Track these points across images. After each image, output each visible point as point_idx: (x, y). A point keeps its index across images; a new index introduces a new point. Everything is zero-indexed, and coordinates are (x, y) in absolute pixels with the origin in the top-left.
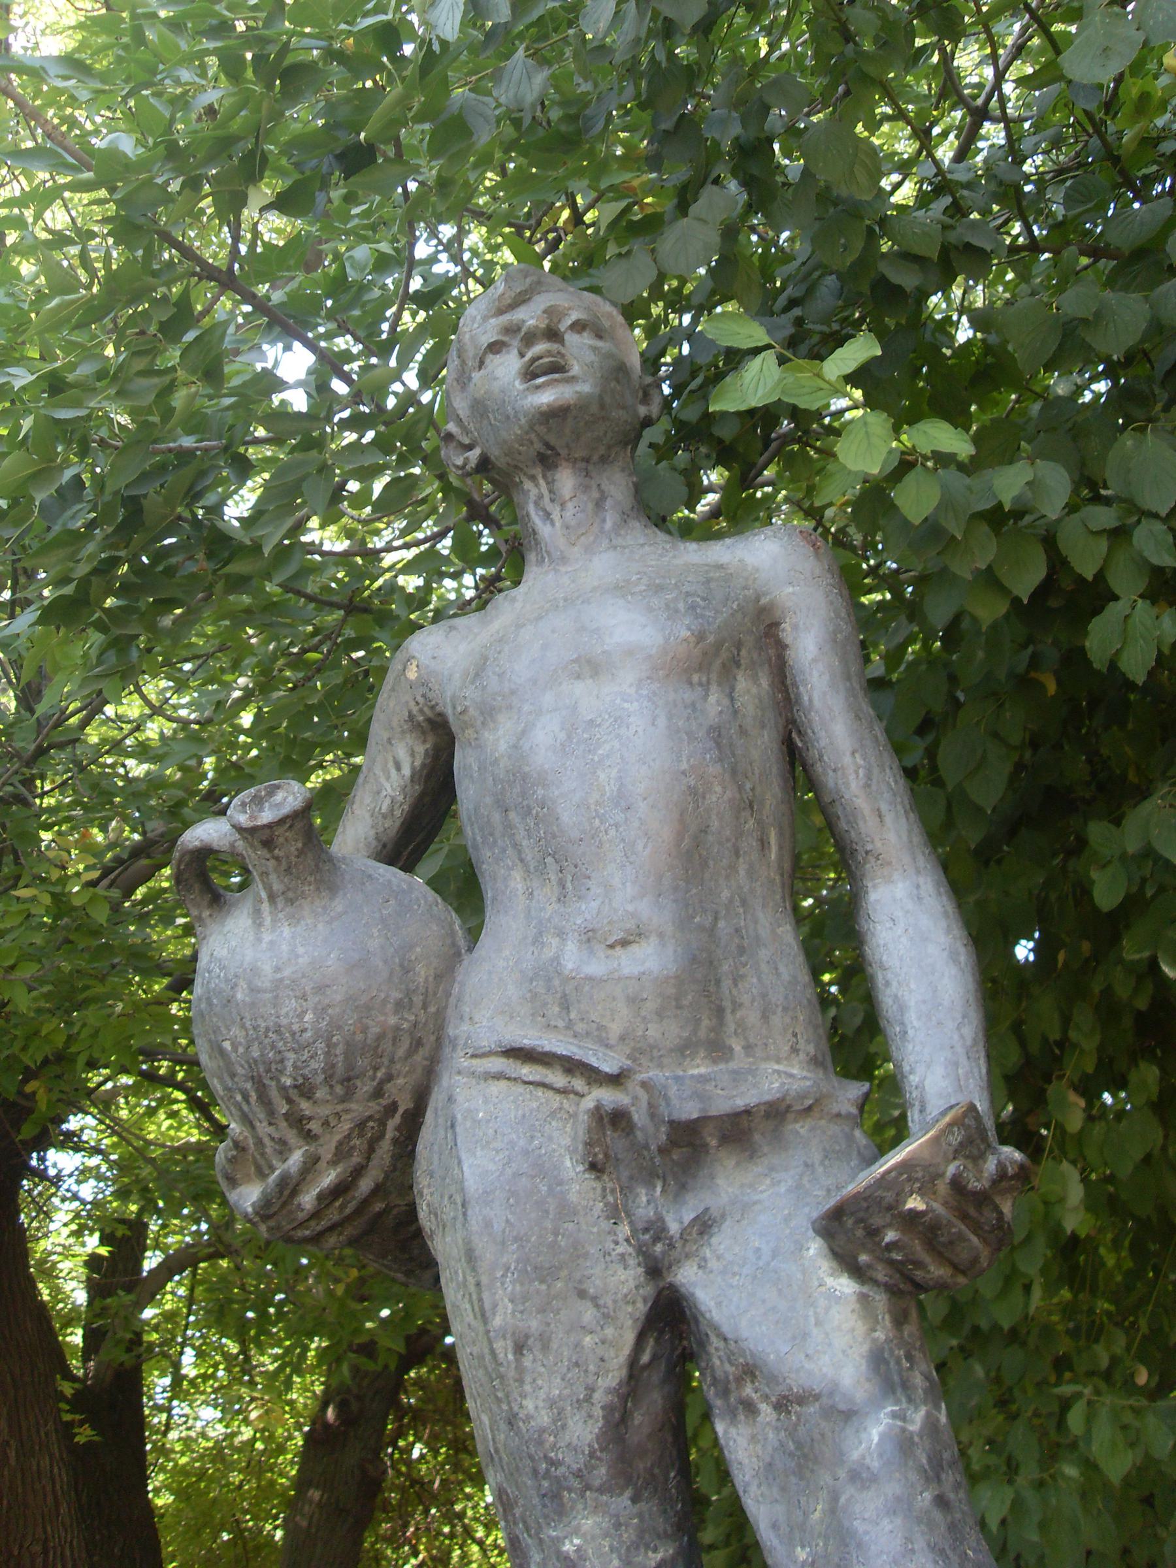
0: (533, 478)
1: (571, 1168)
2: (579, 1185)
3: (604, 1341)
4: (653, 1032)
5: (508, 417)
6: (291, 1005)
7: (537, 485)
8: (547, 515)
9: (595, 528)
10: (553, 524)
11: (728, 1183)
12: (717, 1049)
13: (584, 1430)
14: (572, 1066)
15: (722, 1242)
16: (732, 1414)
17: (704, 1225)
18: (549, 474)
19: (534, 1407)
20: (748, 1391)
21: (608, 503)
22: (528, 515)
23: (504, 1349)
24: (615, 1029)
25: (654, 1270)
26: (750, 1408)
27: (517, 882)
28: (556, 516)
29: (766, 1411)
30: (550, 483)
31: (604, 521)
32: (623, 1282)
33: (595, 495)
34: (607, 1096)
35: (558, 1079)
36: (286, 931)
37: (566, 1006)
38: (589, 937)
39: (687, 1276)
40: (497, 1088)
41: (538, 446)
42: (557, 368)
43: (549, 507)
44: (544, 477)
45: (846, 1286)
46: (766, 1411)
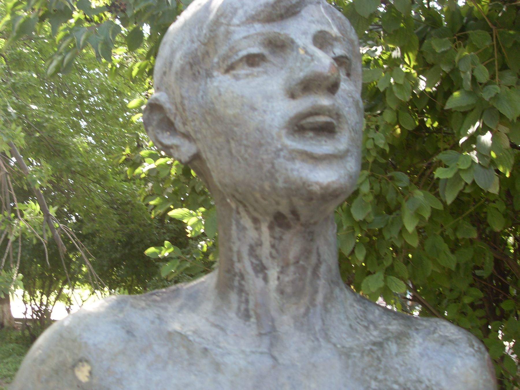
0: (255, 221)
5: (260, 167)
7: (257, 229)
8: (261, 269)
9: (305, 300)
10: (266, 279)
18: (277, 229)
21: (323, 269)
22: (239, 253)
28: (273, 273)
30: (276, 240)
31: (316, 292)
33: (313, 260)
41: (284, 208)
42: (327, 130)
43: (267, 262)
44: (271, 227)
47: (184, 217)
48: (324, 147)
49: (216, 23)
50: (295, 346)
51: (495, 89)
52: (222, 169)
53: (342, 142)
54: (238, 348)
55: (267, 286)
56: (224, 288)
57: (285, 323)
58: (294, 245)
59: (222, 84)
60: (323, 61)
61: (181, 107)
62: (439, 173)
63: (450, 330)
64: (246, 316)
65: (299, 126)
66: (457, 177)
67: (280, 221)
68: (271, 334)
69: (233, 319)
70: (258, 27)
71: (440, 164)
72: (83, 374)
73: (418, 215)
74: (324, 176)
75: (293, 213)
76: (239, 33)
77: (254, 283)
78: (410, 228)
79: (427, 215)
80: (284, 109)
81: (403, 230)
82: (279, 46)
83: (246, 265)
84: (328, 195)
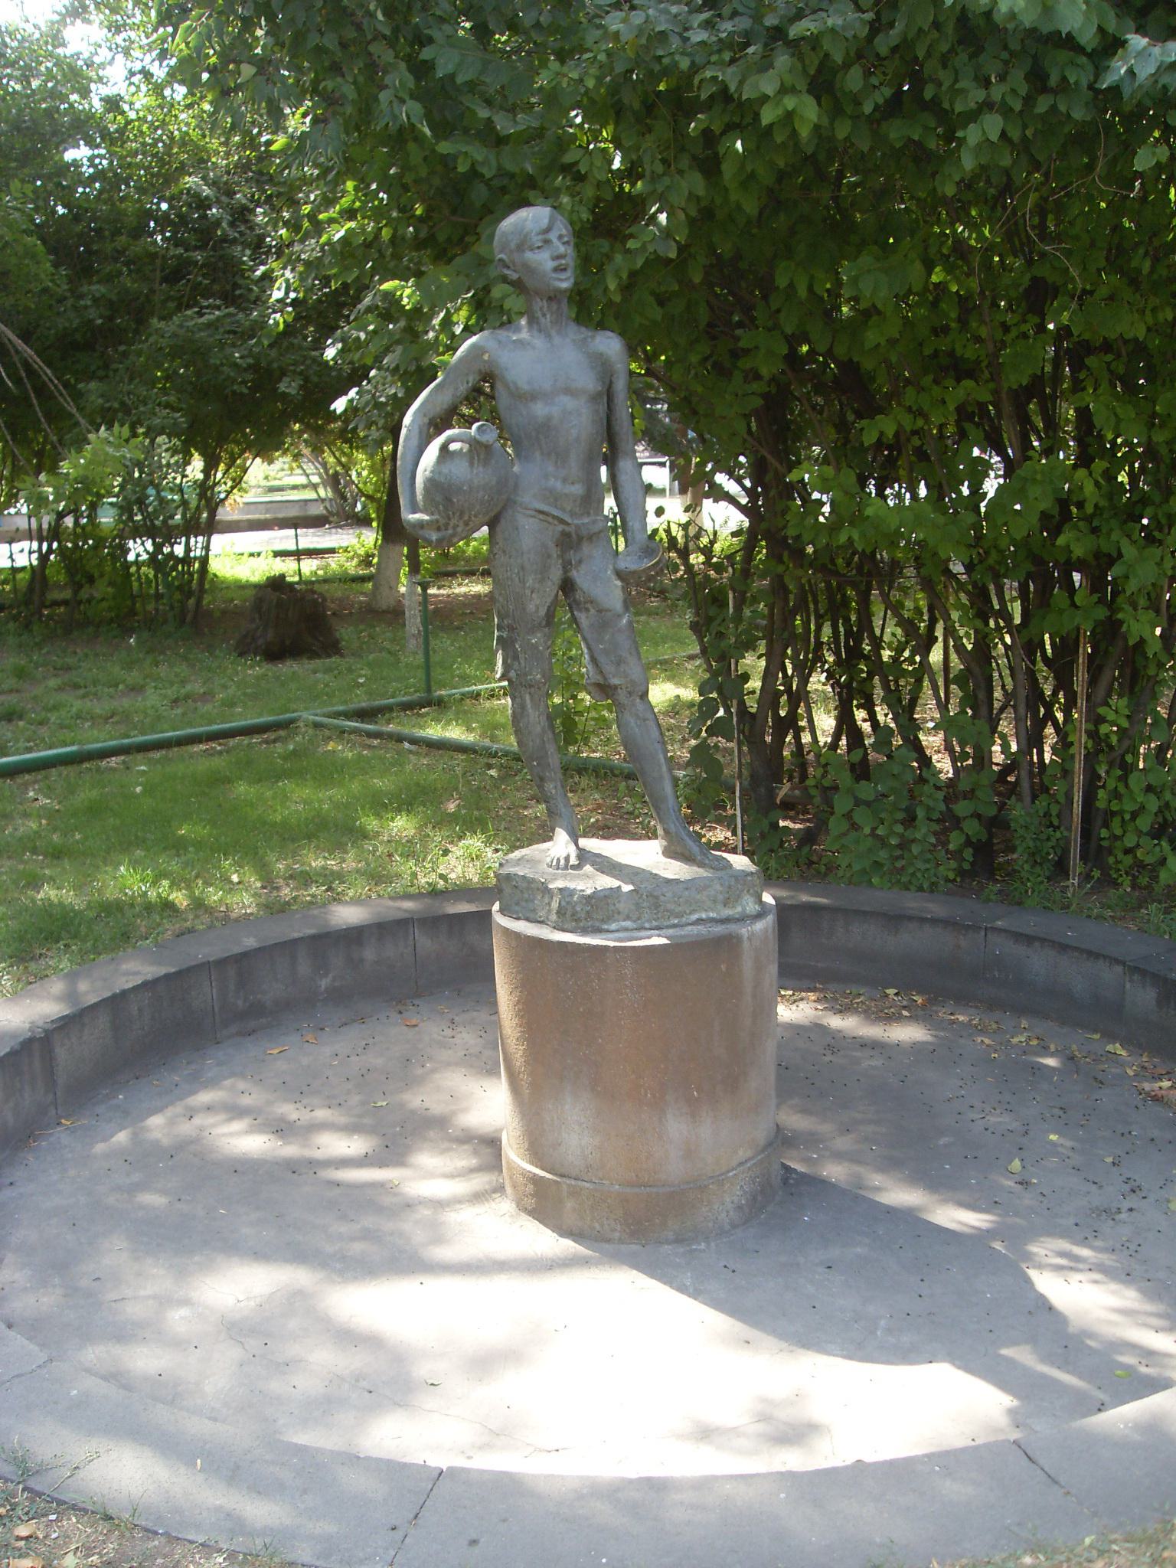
1: (551, 545)
2: (554, 552)
3: (551, 588)
4: (577, 510)
6: (481, 493)
8: (544, 315)
11: (586, 548)
12: (589, 514)
13: (542, 612)
14: (554, 517)
15: (583, 566)
16: (580, 610)
17: (580, 562)
19: (531, 607)
20: (588, 606)
23: (528, 592)
24: (569, 508)
25: (566, 570)
26: (587, 610)
27: (537, 454)
29: (592, 611)
32: (556, 574)
34: (567, 529)
35: (550, 519)
36: (481, 469)
37: (556, 500)
38: (565, 480)
39: (574, 574)
40: (531, 520)
42: (565, 270)
45: (619, 583)
46: (592, 611)
47: (396, 289)
48: (563, 276)
49: (526, 236)
50: (557, 340)
51: (667, 181)
52: (529, 283)
53: (569, 273)
54: (539, 342)
55: (546, 321)
56: (530, 323)
57: (553, 333)
58: (555, 306)
59: (529, 255)
60: (562, 249)
61: (514, 263)
62: (631, 244)
63: (610, 334)
64: (540, 331)
65: (556, 270)
66: (644, 245)
67: (550, 299)
68: (549, 336)
69: (535, 333)
70: (540, 237)
71: (631, 236)
72: (486, 357)
73: (617, 275)
74: (565, 285)
75: (553, 297)
76: (535, 239)
77: (543, 320)
78: (612, 285)
79: (625, 276)
80: (550, 265)
81: (606, 289)
82: (547, 242)
83: (539, 314)
84: (566, 290)
